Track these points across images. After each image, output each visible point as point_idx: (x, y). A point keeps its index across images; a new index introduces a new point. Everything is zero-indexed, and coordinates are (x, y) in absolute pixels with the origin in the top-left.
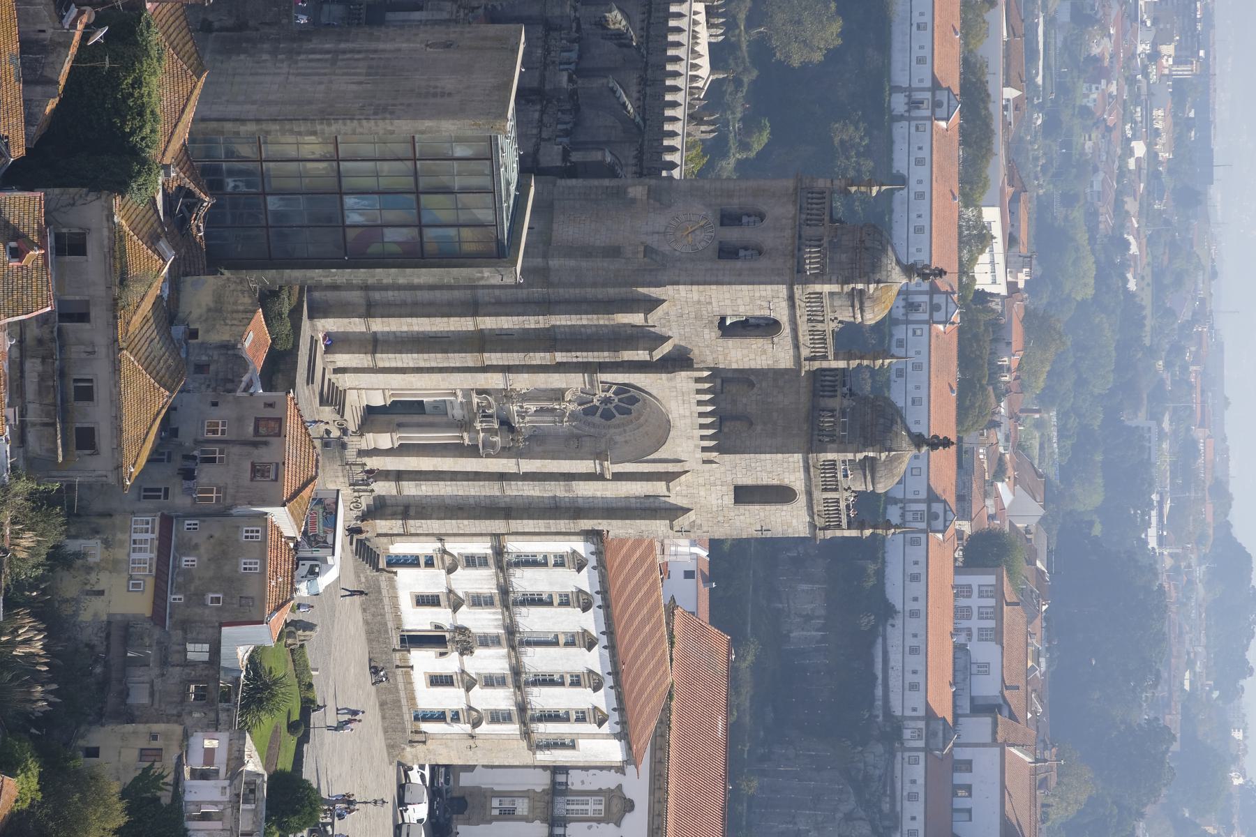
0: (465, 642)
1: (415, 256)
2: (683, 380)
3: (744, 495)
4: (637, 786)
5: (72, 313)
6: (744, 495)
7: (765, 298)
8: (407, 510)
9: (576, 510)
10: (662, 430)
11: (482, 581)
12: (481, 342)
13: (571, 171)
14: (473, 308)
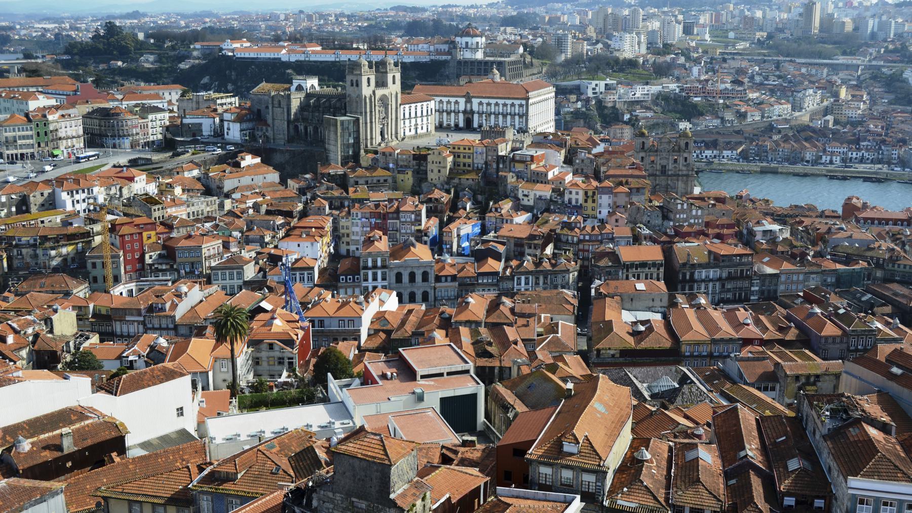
0: (416, 125)
1: (358, 131)
2: (377, 92)
3: (394, 83)
4: (438, 99)
5: (367, 183)
6: (394, 83)
7: (364, 80)
8: (396, 133)
9: (397, 108)
10: (384, 96)
11: (407, 122)
12: (371, 122)
13: (345, 108)
14: (366, 123)
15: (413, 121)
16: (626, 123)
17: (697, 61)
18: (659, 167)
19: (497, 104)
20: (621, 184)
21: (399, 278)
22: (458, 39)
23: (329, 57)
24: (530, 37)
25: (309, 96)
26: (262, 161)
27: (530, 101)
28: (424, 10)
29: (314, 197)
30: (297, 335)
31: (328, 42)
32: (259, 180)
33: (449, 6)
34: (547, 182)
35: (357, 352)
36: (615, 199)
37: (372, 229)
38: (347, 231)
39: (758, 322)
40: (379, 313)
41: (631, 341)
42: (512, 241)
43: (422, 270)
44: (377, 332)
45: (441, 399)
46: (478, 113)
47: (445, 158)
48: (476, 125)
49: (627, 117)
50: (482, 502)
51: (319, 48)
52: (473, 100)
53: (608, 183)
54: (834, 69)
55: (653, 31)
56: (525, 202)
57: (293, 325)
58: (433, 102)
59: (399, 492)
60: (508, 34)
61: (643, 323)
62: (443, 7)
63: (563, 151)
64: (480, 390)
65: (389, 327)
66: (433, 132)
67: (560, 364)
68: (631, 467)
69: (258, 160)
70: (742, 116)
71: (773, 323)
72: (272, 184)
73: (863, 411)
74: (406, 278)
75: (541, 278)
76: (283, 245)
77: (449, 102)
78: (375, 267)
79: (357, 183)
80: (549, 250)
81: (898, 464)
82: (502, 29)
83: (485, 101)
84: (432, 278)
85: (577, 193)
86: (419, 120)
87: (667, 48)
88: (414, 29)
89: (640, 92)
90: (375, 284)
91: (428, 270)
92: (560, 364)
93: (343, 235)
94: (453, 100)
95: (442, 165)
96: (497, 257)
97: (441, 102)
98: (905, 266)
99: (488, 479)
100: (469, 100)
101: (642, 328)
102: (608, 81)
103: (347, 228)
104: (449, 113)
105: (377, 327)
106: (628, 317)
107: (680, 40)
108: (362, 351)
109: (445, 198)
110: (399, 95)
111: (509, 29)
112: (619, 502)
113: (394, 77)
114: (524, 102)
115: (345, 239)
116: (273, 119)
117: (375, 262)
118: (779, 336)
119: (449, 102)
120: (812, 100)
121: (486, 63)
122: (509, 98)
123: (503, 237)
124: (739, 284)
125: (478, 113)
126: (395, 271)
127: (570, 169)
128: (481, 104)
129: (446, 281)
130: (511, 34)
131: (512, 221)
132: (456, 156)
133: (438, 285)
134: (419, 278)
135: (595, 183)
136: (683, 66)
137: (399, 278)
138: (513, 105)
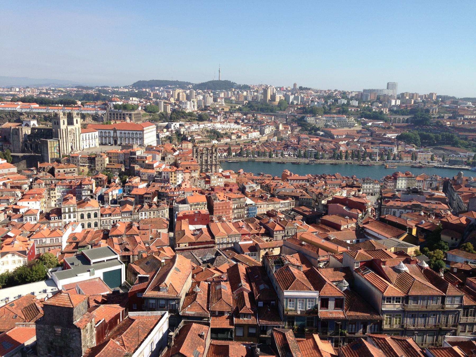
1: (59, 147)
2: (68, 127)
3: (77, 123)
4: (100, 131)
6: (77, 123)
11: (85, 142)
15: (88, 141)
16: (189, 141)
17: (219, 114)
18: (204, 161)
19: (129, 133)
20: (187, 168)
21: (82, 217)
22: (109, 102)
23: (43, 110)
24: (144, 102)
25: (33, 129)
26: (7, 162)
27: (145, 132)
28: (92, 88)
29: (36, 179)
30: (27, 248)
31: (42, 102)
32: (6, 171)
33: (105, 87)
34: (153, 169)
35: (60, 254)
36: (184, 175)
37: (68, 193)
38: (55, 195)
39: (248, 226)
40: (71, 234)
41: (193, 239)
42: (138, 196)
43: (94, 212)
44: (71, 243)
45: (105, 274)
46: (120, 137)
47: (104, 159)
48: (119, 143)
49: (189, 138)
50: (121, 320)
51: (38, 106)
52: (117, 131)
53: (180, 168)
54: (277, 117)
55: (200, 100)
56: (144, 178)
57: (25, 243)
58: (97, 132)
59: (78, 320)
60: (134, 101)
61: (198, 230)
62: (101, 87)
63: (161, 154)
64: (123, 267)
65: (77, 241)
66: (98, 146)
67: (161, 252)
68: (192, 295)
69: (5, 161)
70: (240, 137)
71: (254, 226)
72: (13, 173)
73: (289, 261)
74: (86, 217)
75: (152, 212)
76: (20, 204)
77: (105, 132)
78: (69, 212)
79: (59, 171)
80: (155, 200)
81: (303, 282)
82: (131, 99)
83: (123, 132)
84: (99, 215)
85: (167, 173)
86: (91, 141)
87: (206, 108)
88: (87, 98)
89: (195, 127)
90: (70, 220)
91: (97, 211)
92: (161, 252)
93: (52, 197)
94: (107, 131)
95: (103, 162)
96: (131, 203)
97: (101, 132)
98: (307, 199)
99: (124, 308)
100: (115, 131)
101: (198, 232)
102: (181, 123)
103: (55, 193)
104: (105, 138)
105: (71, 241)
106: (192, 227)
107: (212, 104)
108: (63, 253)
109: (105, 177)
110: (80, 129)
111: (134, 99)
112: (187, 312)
113: (77, 120)
114: (141, 132)
115: (54, 199)
116: (13, 141)
117: (69, 209)
118: (257, 231)
119: (105, 132)
120: (268, 130)
121: (124, 114)
122: (134, 131)
123: (134, 195)
124: (240, 210)
125: (120, 137)
126: (80, 214)
127: (163, 162)
128: (121, 133)
129: (106, 216)
130: (135, 101)
131: (137, 187)
132: (110, 158)
133: (102, 218)
134: (92, 216)
135: (175, 168)
136: (213, 116)
137: (82, 217)
138: (136, 134)
